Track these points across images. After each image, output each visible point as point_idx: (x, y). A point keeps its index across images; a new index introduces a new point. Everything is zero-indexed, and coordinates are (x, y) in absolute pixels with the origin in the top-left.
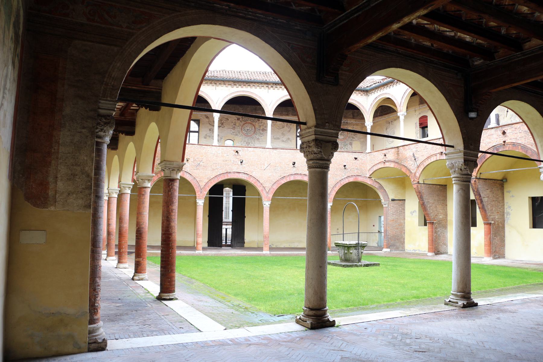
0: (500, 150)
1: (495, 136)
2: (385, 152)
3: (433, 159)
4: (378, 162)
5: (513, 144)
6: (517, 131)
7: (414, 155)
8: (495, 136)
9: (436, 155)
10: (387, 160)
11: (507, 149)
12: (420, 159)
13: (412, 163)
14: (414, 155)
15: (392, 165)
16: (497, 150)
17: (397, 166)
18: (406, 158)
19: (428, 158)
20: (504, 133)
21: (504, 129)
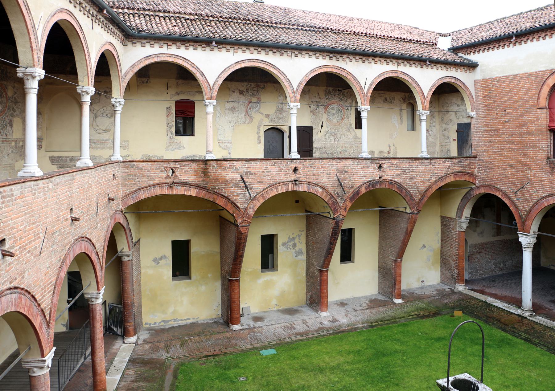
0: (377, 187)
1: (371, 169)
2: (172, 165)
3: (282, 189)
4: (151, 183)
5: (391, 182)
6: (394, 168)
7: (242, 178)
8: (371, 169)
9: (286, 183)
10: (176, 181)
11: (384, 186)
12: (256, 187)
13: (239, 191)
14: (242, 178)
15: (193, 192)
16: (373, 186)
17: (203, 194)
18: (226, 183)
19: (272, 186)
20: (380, 167)
21: (381, 162)
